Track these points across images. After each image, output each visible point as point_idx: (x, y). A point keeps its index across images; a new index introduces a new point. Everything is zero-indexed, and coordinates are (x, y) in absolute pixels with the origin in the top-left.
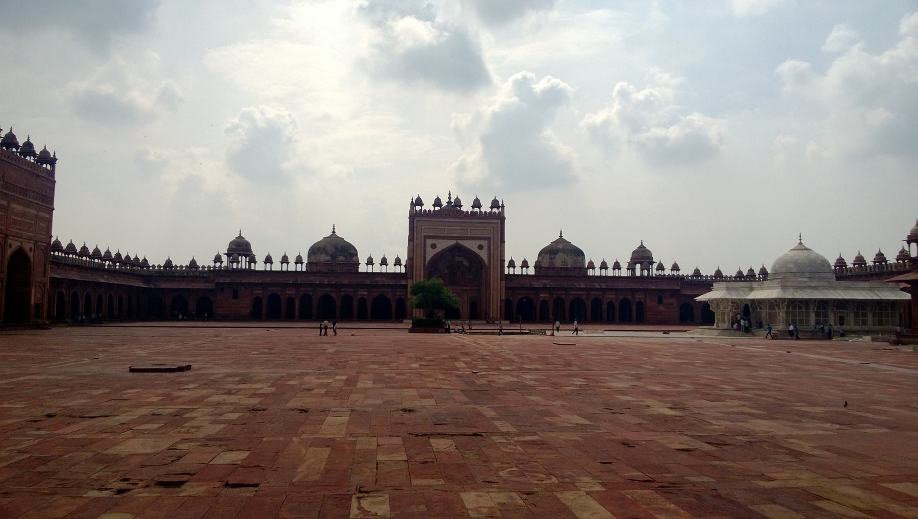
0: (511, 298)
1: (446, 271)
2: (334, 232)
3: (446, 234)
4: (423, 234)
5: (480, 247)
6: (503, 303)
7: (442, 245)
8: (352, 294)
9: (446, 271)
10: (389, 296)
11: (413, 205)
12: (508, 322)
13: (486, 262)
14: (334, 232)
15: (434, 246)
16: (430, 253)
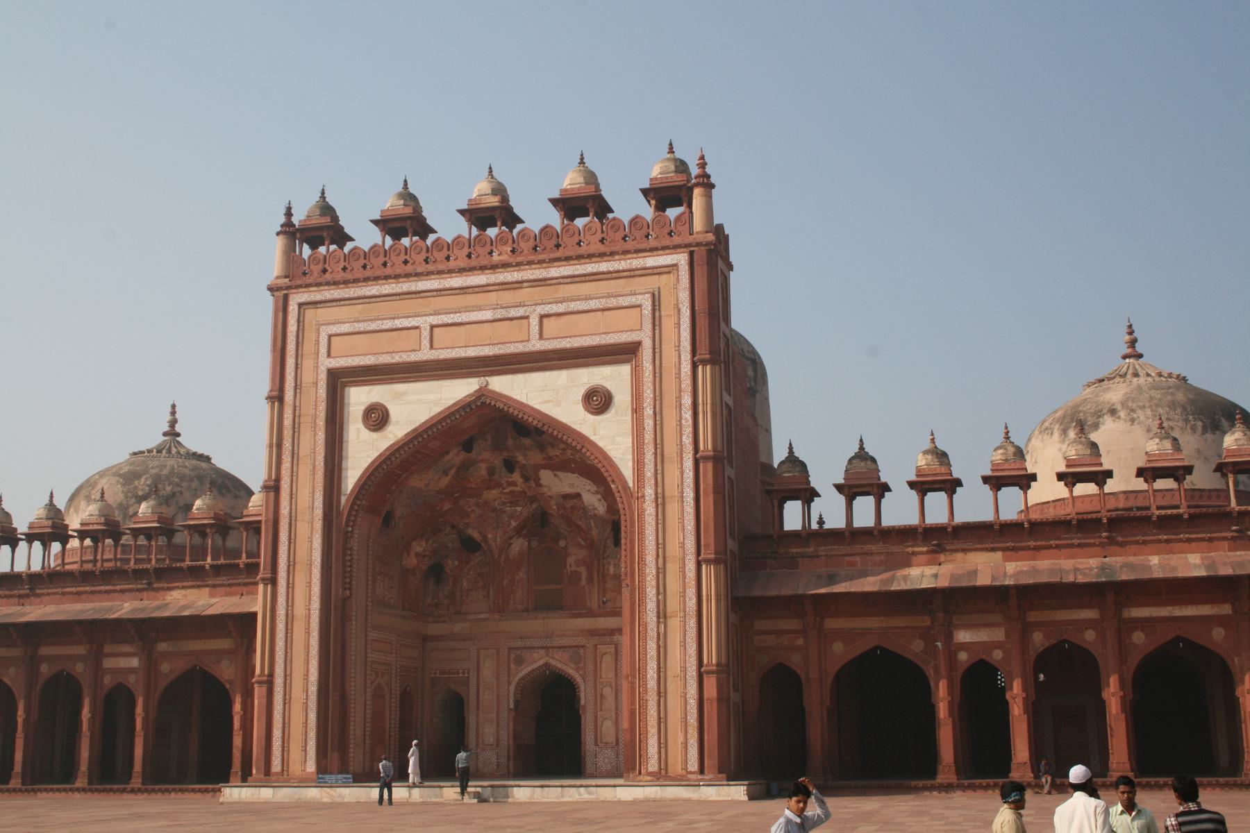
0: (795, 660)
1: (518, 545)
2: (172, 433)
3: (426, 354)
4: (328, 363)
5: (598, 401)
6: (711, 690)
7: (416, 406)
8: (79, 667)
9: (518, 545)
10: (226, 671)
11: (290, 231)
12: (738, 792)
13: (627, 471)
14: (172, 433)
15: (377, 418)
16: (363, 450)
